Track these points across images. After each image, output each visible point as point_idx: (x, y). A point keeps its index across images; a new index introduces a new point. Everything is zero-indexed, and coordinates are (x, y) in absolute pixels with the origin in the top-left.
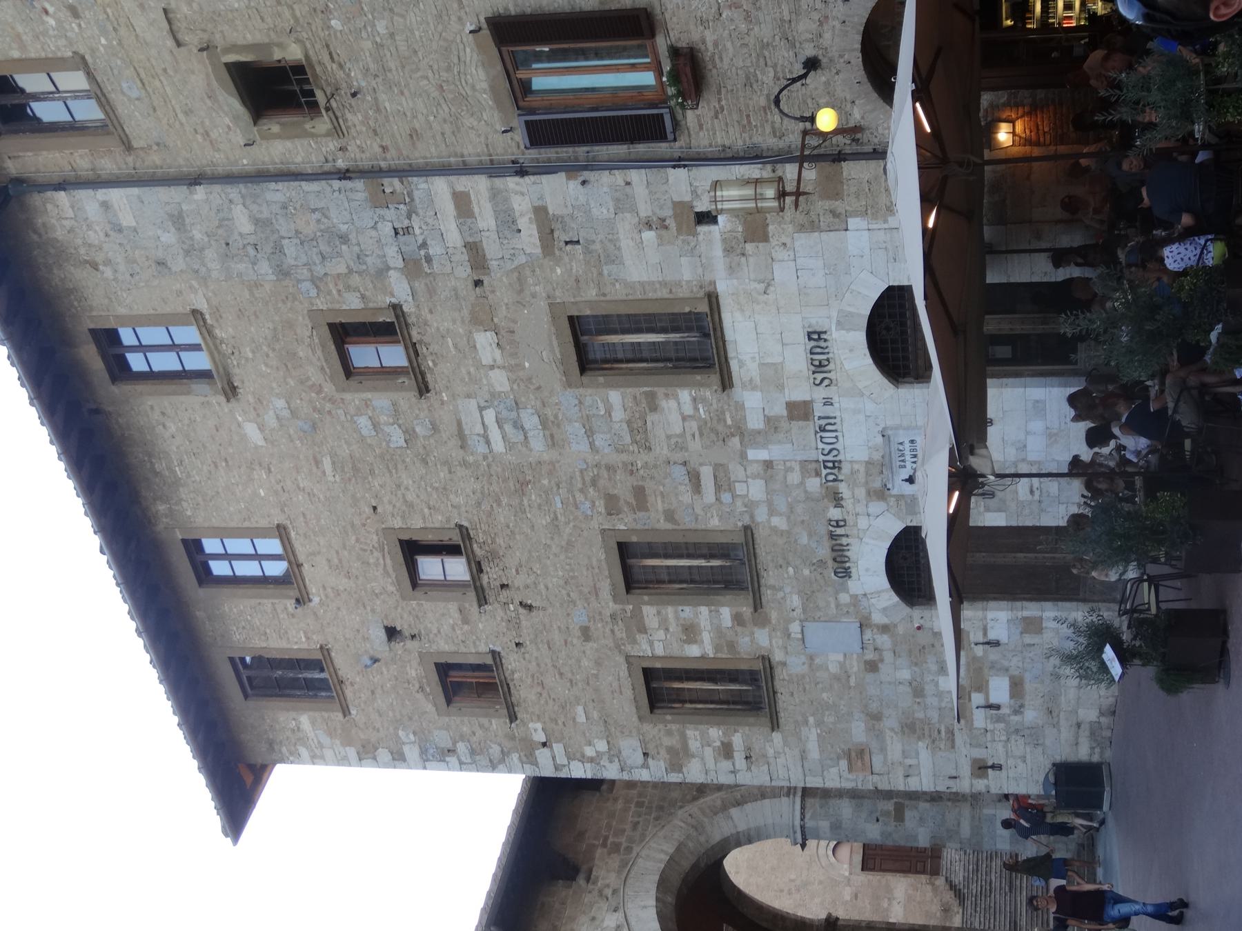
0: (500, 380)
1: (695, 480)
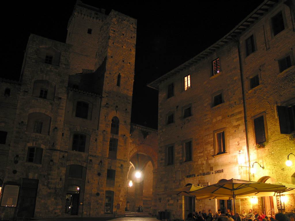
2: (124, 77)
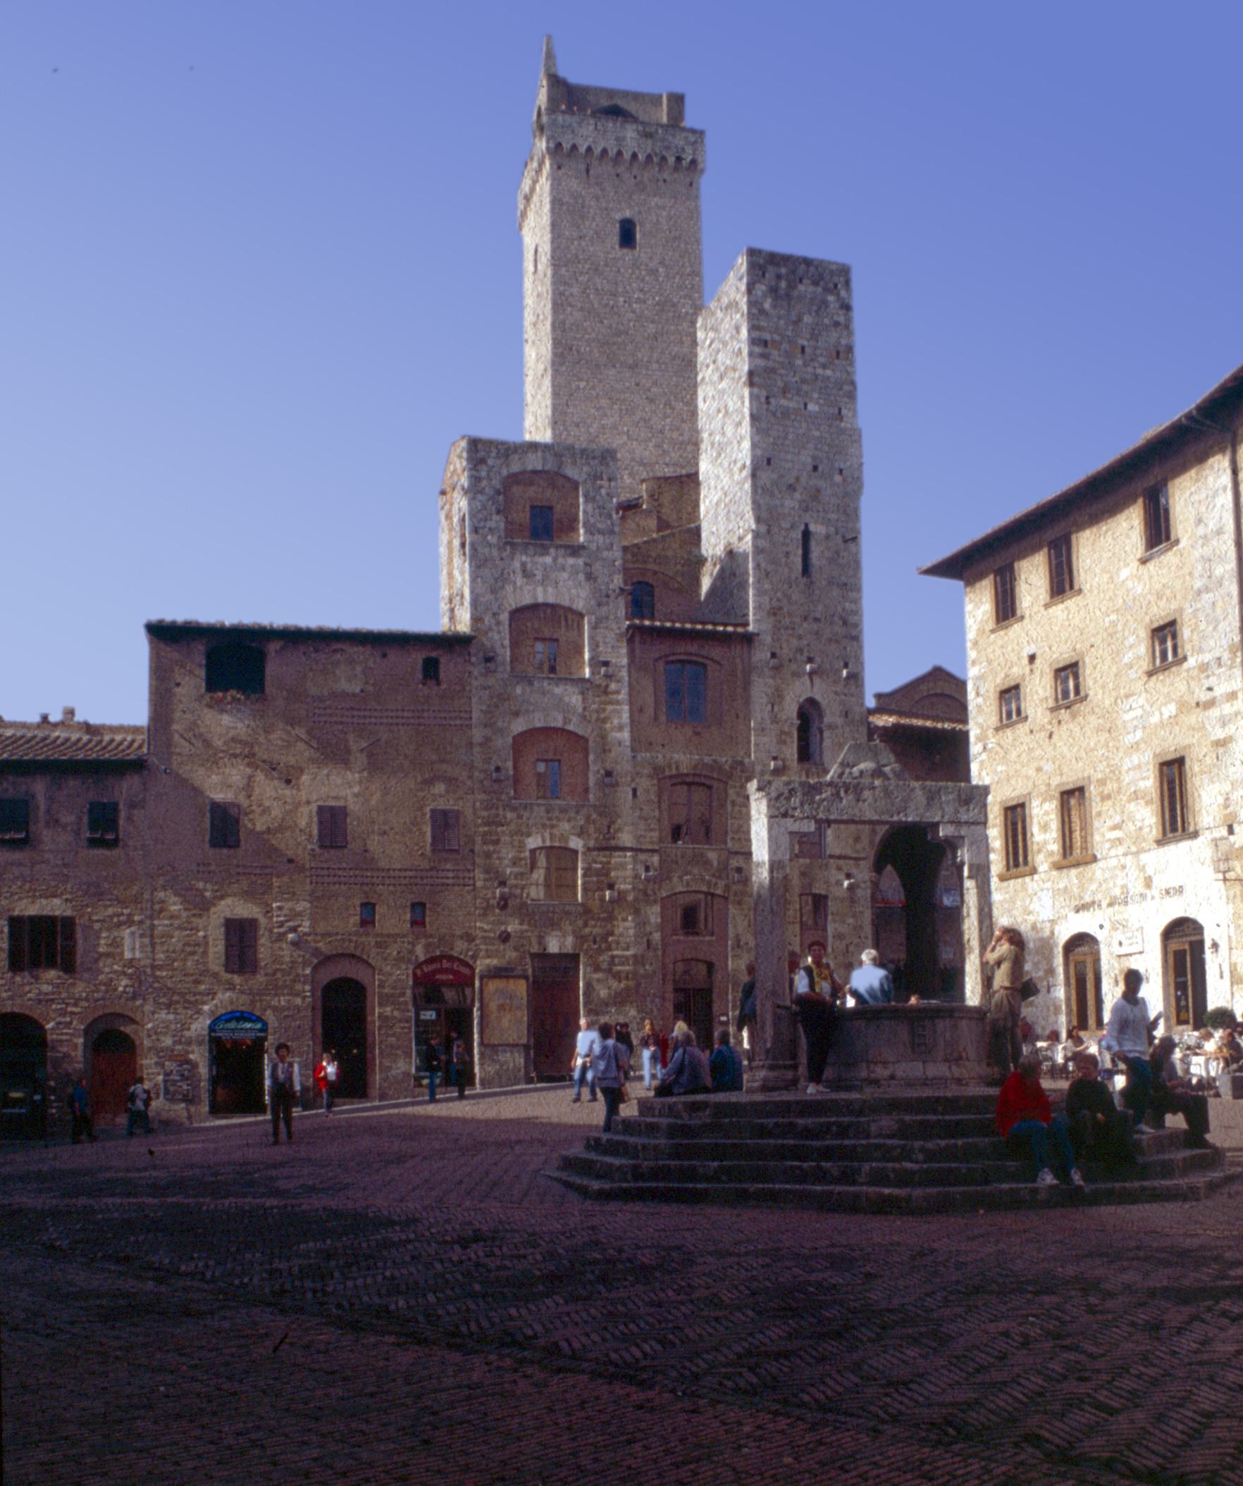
0: (1155, 719)
1: (1116, 827)
2: (827, 537)
